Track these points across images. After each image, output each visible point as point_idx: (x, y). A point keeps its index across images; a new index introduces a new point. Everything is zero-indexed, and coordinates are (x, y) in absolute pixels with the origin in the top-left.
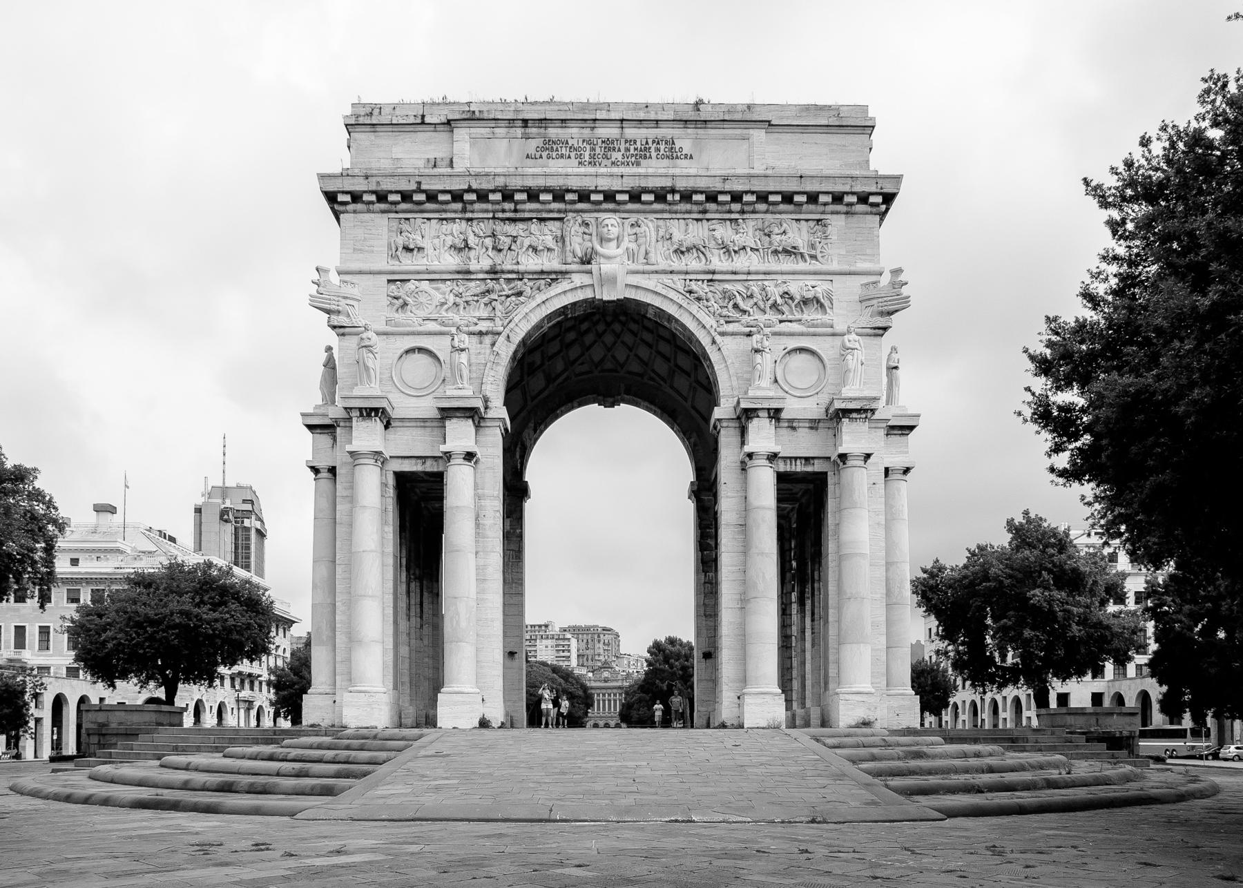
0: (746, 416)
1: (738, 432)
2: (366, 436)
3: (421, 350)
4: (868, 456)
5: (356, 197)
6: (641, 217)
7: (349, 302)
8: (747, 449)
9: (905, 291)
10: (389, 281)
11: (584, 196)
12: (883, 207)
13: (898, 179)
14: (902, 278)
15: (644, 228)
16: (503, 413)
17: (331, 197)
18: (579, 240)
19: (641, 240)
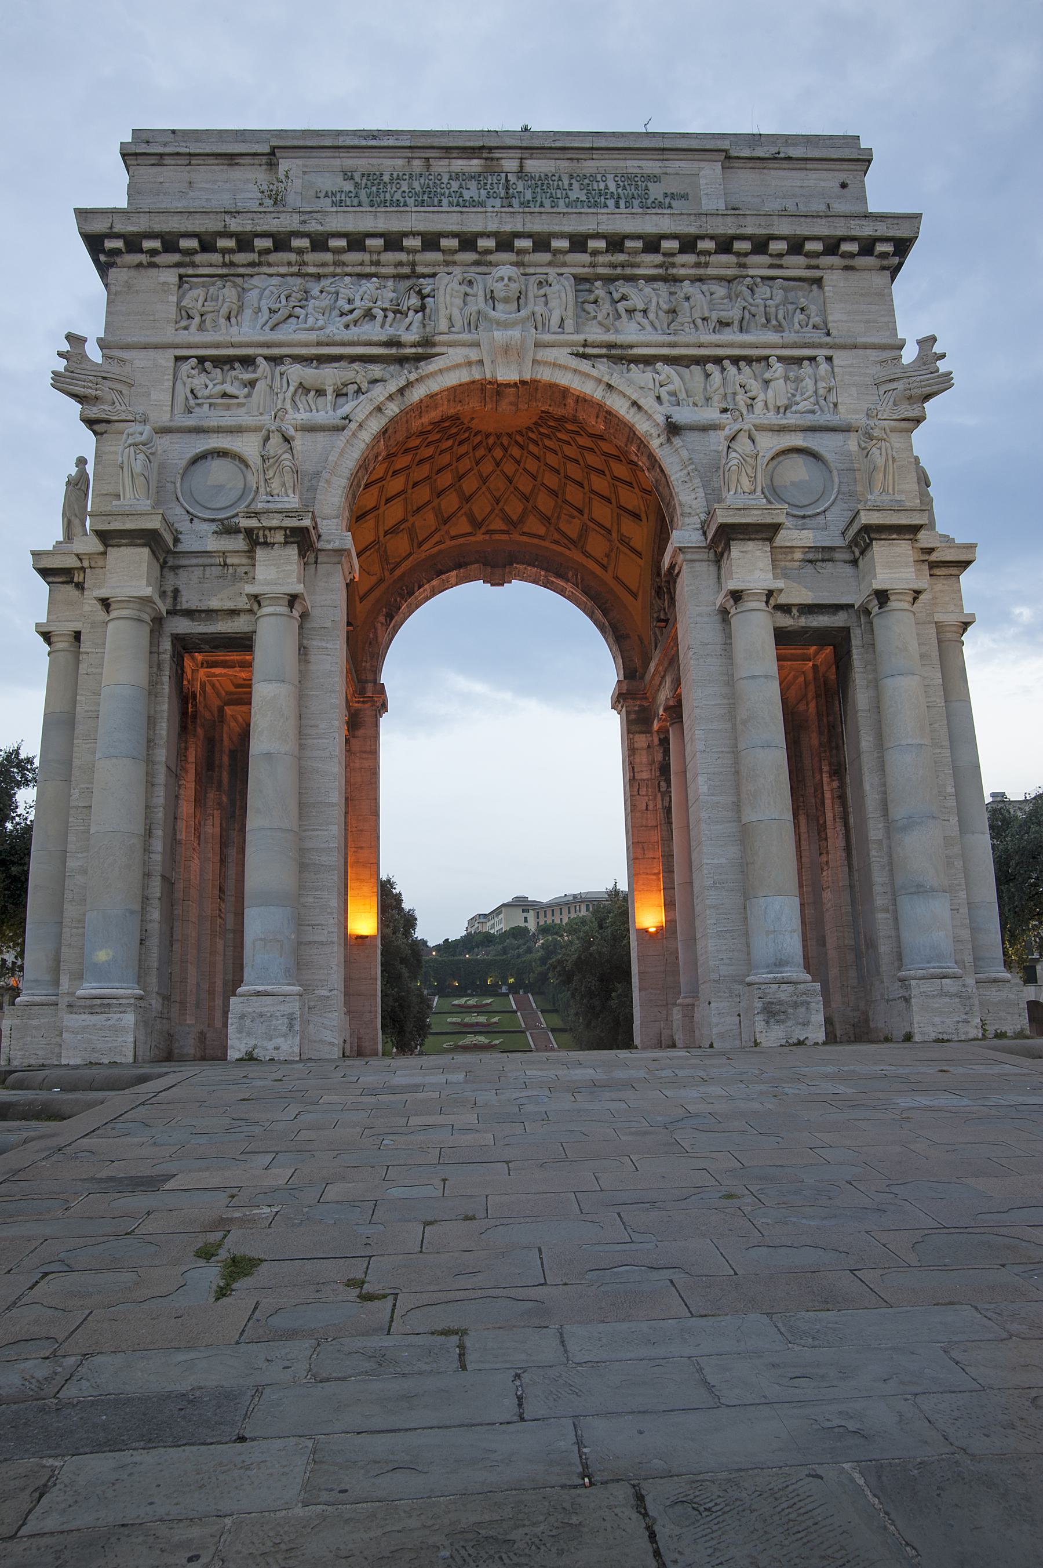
0: (724, 538)
1: (713, 568)
2: (129, 574)
3: (221, 453)
4: (918, 593)
5: (133, 243)
6: (552, 271)
7: (118, 386)
9: (942, 366)
10: (178, 359)
11: (468, 242)
12: (896, 260)
13: (915, 218)
14: (937, 349)
15: (556, 287)
16: (347, 541)
17: (94, 243)
18: (459, 302)
19: (553, 303)
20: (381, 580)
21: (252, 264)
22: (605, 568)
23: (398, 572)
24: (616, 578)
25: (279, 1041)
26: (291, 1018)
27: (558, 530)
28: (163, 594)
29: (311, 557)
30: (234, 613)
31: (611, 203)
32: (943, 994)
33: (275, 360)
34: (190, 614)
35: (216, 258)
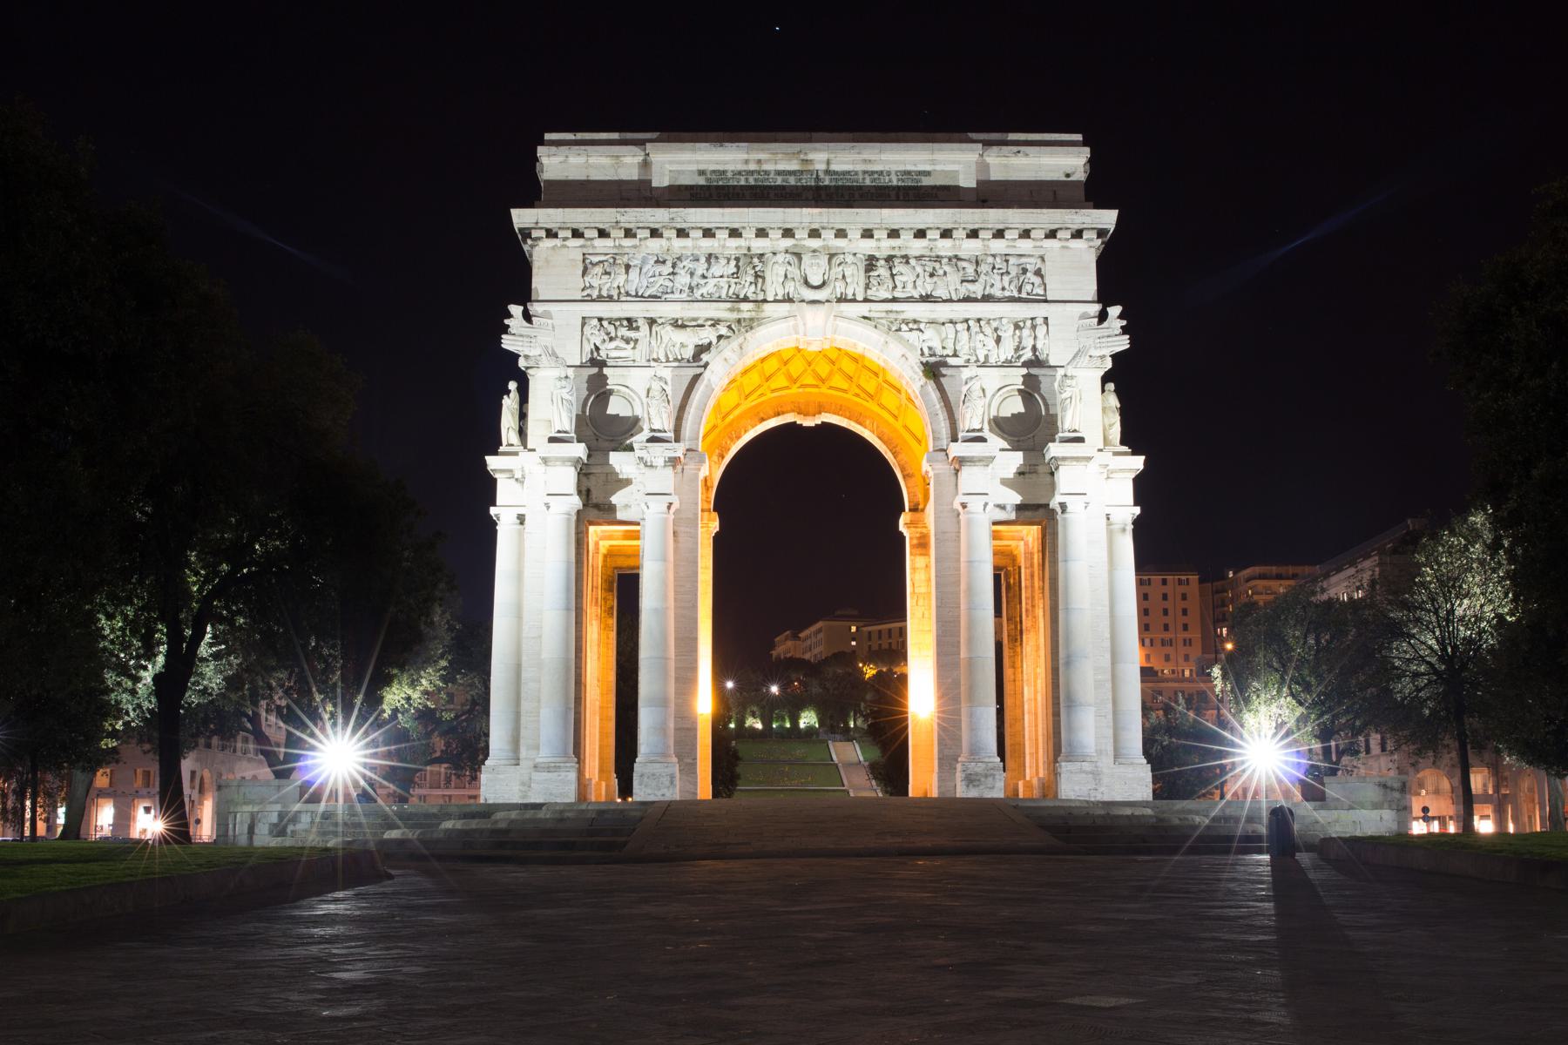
8: (960, 499)
20: (715, 427)
21: (635, 247)
22: (895, 417)
23: (728, 420)
24: (905, 426)
25: (664, 791)
26: (672, 777)
27: (859, 386)
28: (579, 492)
29: (679, 467)
30: (627, 506)
31: (893, 194)
32: (1082, 771)
33: (652, 322)
34: (597, 506)
35: (607, 242)
